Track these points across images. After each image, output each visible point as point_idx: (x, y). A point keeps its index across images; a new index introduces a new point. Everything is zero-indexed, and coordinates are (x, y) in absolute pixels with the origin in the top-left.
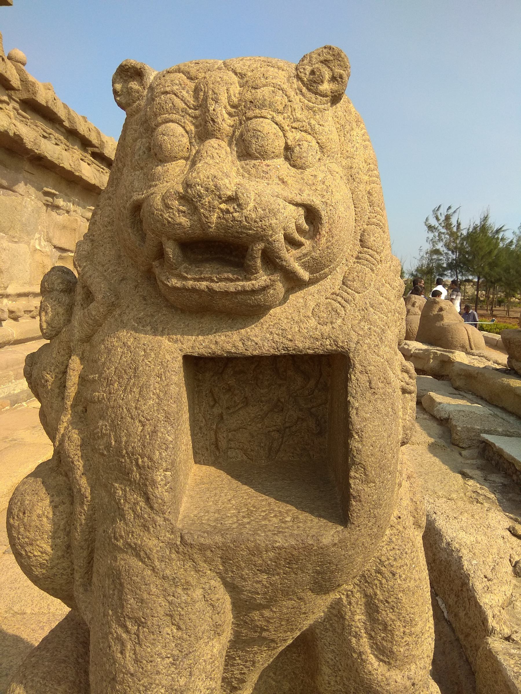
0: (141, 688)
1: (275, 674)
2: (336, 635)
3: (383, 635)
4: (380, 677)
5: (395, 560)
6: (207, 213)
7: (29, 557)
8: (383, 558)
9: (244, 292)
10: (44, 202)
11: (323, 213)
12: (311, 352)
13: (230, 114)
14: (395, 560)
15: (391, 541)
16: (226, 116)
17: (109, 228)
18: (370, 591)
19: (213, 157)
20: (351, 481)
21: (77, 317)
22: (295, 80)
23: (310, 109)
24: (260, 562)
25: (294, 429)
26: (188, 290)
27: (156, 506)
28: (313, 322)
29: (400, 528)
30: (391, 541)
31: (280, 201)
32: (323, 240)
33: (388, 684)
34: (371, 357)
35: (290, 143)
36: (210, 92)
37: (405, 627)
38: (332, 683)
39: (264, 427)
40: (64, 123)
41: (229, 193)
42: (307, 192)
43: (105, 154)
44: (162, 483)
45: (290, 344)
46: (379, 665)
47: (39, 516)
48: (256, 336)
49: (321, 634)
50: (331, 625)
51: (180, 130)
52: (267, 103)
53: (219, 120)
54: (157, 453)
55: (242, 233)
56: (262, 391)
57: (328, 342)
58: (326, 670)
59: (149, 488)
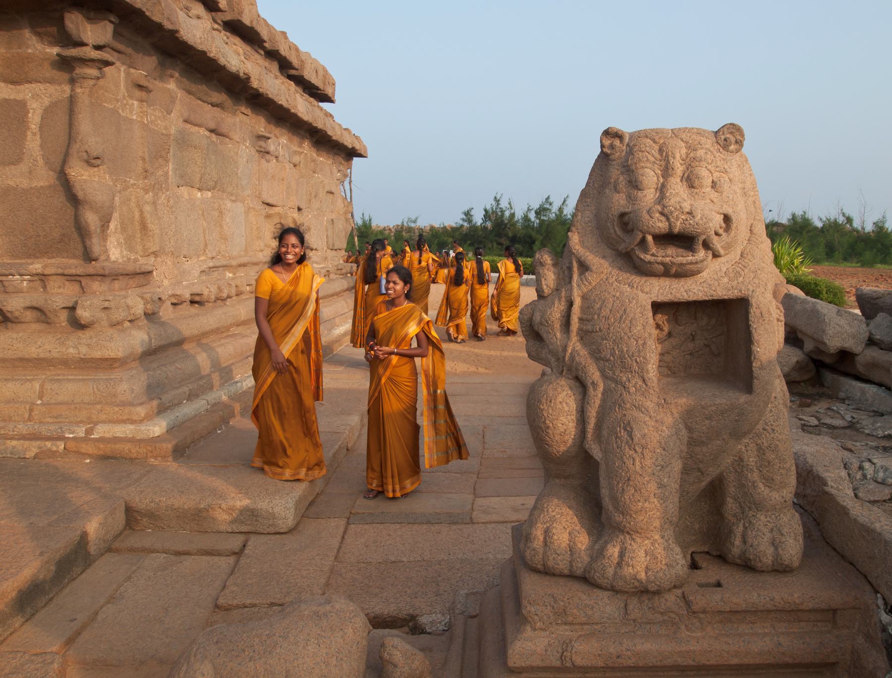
0: (645, 482)
1: (689, 517)
2: (737, 474)
3: (767, 469)
4: (766, 496)
5: (774, 422)
6: (675, 222)
7: (555, 428)
8: (767, 421)
9: (691, 263)
10: (258, 148)
11: (733, 217)
12: (726, 297)
13: (681, 164)
14: (774, 422)
15: (771, 411)
16: (679, 165)
17: (589, 224)
18: (759, 442)
19: (674, 190)
20: (754, 369)
21: (575, 281)
22: (716, 144)
23: (724, 160)
24: (707, 412)
25: (700, 352)
26: (658, 263)
27: (649, 384)
28: (726, 280)
29: (776, 403)
30: (771, 411)
31: (713, 213)
32: (733, 232)
33: (771, 500)
34: (760, 298)
35: (714, 180)
36: (670, 153)
37: (780, 463)
38: (734, 508)
39: (681, 352)
40: (265, 44)
41: (687, 210)
42: (725, 206)
43: (305, 77)
44: (652, 371)
45: (714, 293)
46: (765, 489)
47: (561, 402)
48: (694, 289)
49: (727, 475)
50: (734, 468)
51: (652, 173)
52: (703, 159)
53: (676, 168)
54: (648, 355)
55: (694, 231)
56: (680, 327)
57: (736, 291)
58: (729, 500)
59: (645, 374)
